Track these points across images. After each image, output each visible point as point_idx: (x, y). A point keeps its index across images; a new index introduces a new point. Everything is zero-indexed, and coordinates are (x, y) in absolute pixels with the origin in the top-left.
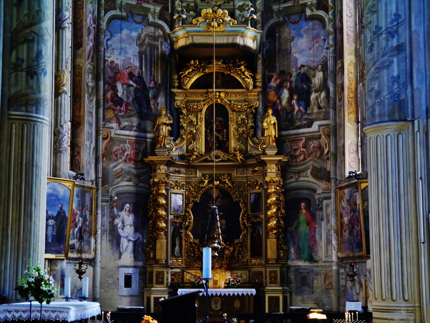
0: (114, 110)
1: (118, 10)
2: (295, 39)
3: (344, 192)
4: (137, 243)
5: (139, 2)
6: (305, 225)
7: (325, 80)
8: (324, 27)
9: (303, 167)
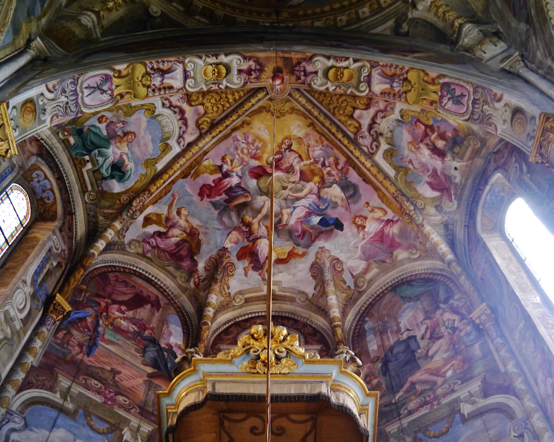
1: (58, 395)
5: (109, 403)
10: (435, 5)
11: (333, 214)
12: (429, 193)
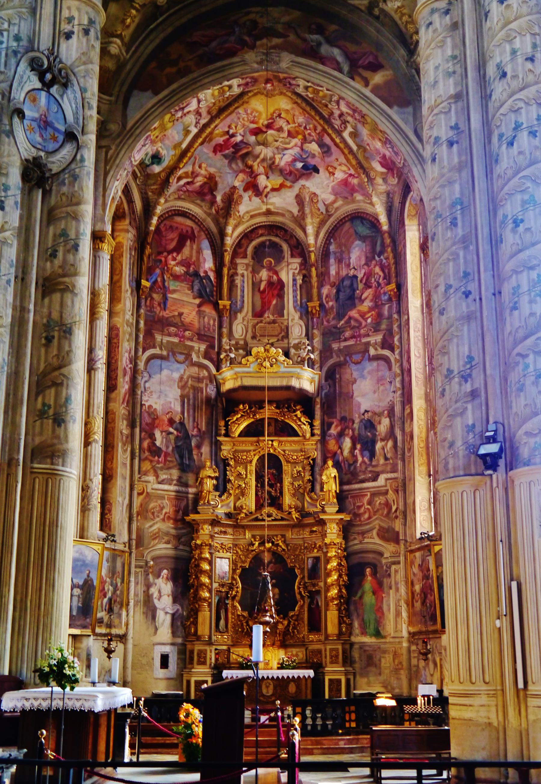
0: (151, 461)
2: (358, 381)
3: (415, 556)
4: (175, 617)
6: (371, 594)
7: (392, 427)
8: (390, 369)
9: (367, 527)
10: (401, 11)
11: (312, 162)
12: (379, 169)
